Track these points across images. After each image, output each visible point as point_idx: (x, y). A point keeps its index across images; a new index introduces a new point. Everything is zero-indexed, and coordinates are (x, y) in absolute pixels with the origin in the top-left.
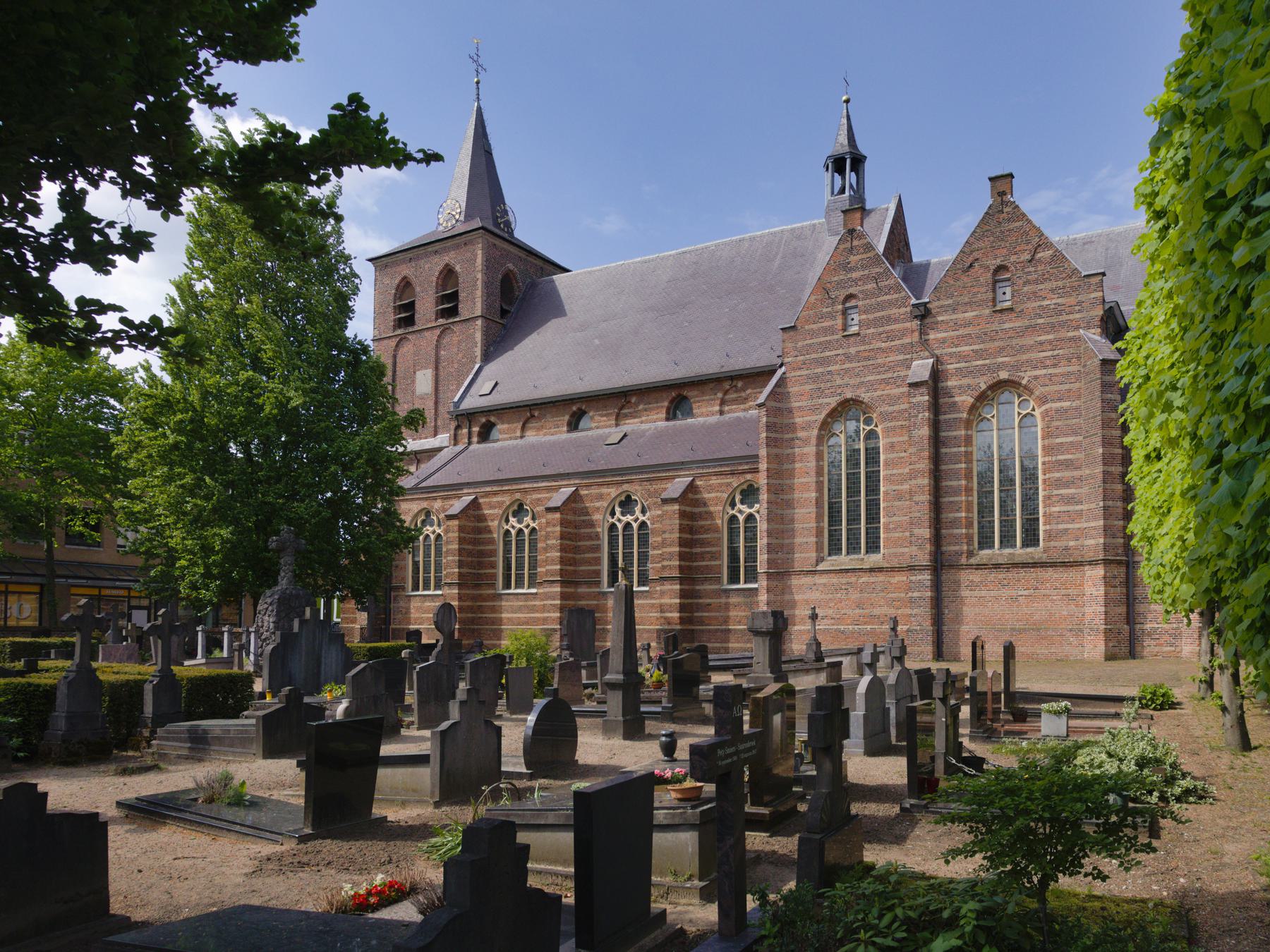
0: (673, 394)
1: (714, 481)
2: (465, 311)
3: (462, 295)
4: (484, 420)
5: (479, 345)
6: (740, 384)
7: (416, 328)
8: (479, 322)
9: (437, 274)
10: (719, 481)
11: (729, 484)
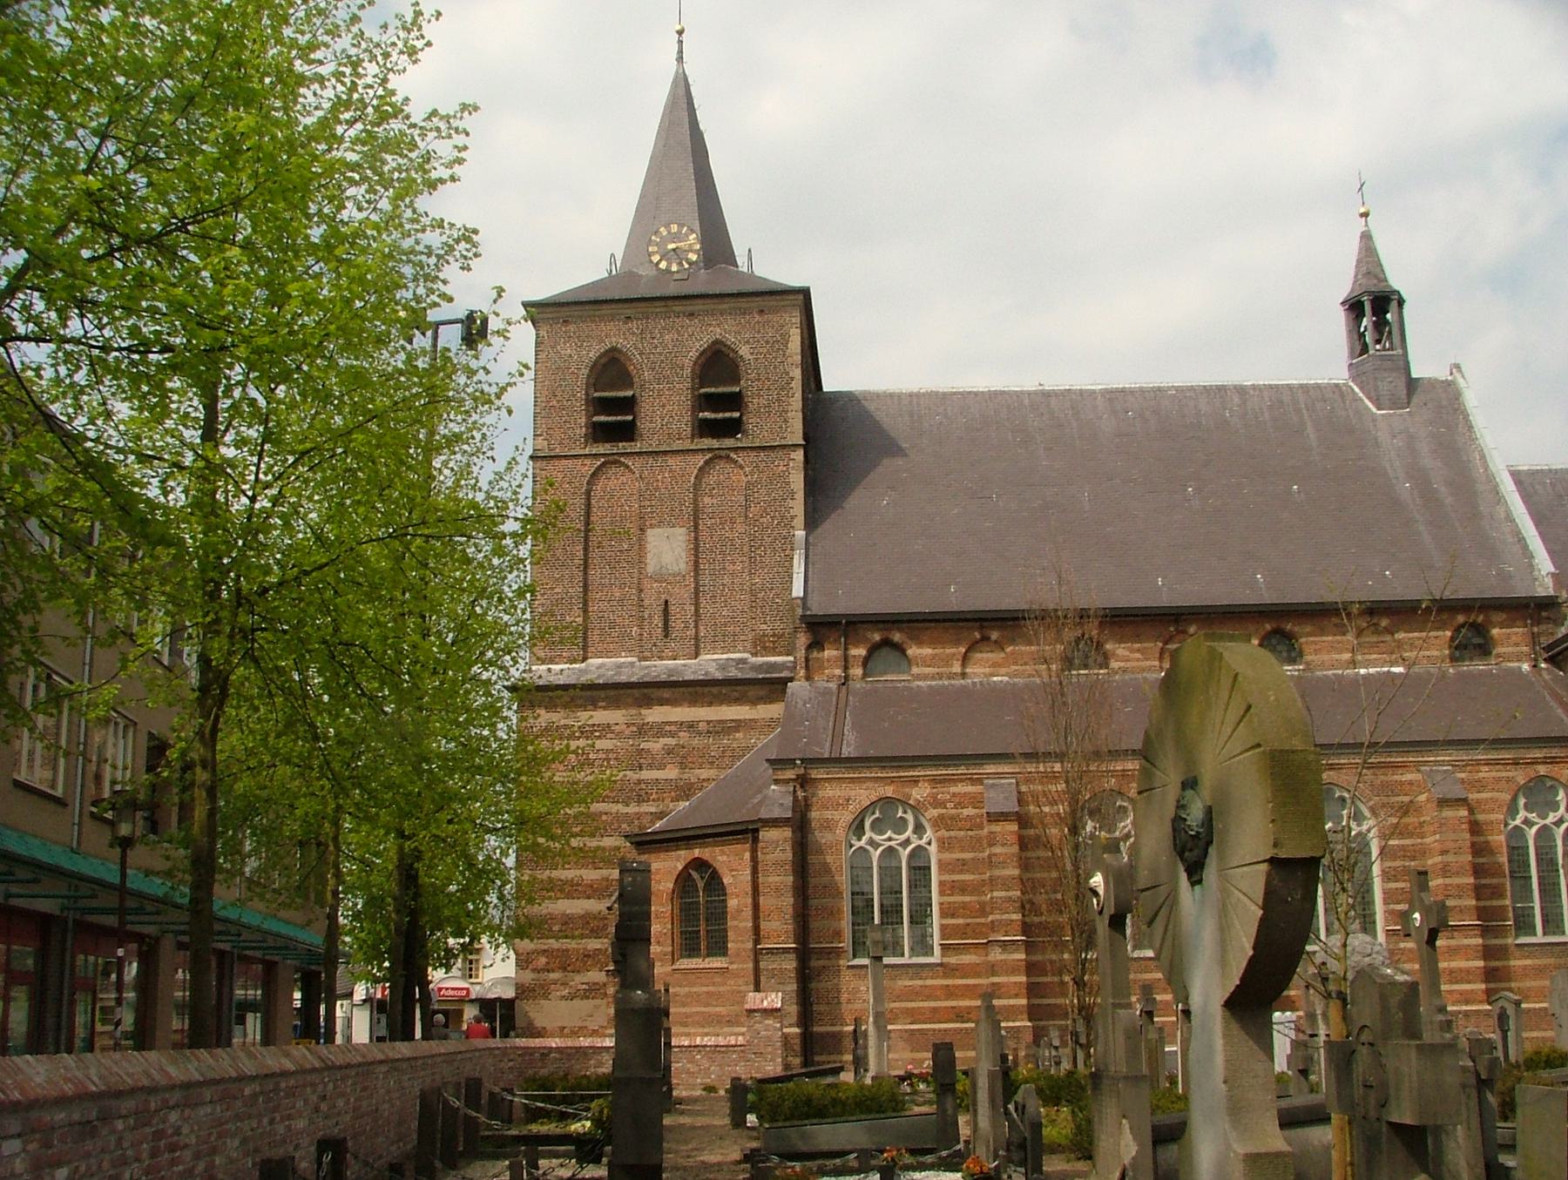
0: (1268, 627)
1: (1485, 773)
2: (758, 428)
3: (753, 403)
4: (877, 637)
5: (800, 496)
6: (1384, 622)
7: (637, 446)
8: (799, 455)
9: (693, 354)
10: (1494, 774)
11: (1508, 780)
